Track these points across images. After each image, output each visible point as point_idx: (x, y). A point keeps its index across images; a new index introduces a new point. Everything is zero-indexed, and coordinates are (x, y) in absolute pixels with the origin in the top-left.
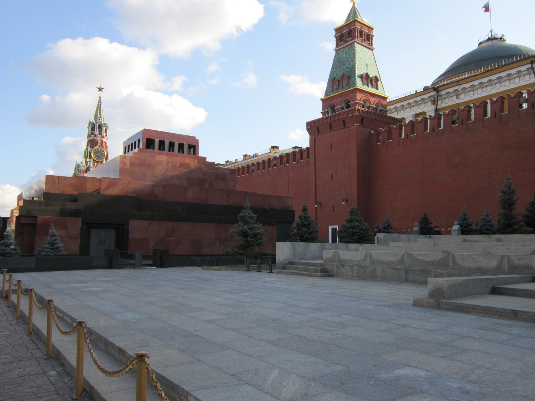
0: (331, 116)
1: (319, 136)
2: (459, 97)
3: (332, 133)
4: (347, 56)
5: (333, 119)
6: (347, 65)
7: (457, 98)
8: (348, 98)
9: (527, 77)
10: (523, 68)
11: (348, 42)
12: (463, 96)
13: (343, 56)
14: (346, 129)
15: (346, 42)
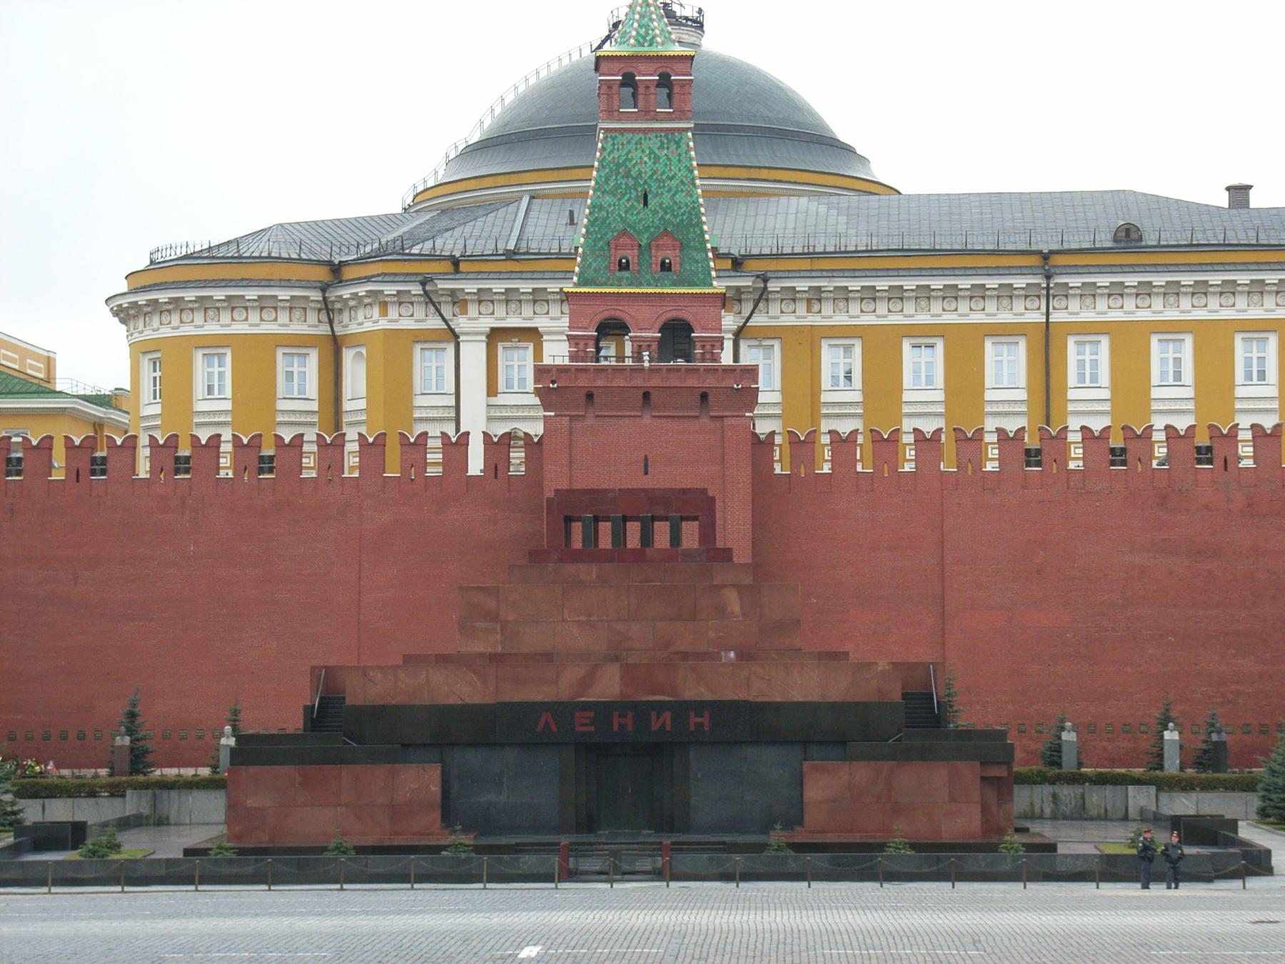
0: (651, 370)
1: (590, 421)
2: (816, 307)
3: (647, 420)
4: (660, 167)
5: (654, 382)
6: (666, 199)
7: (809, 311)
8: (688, 314)
9: (1019, 306)
10: (1019, 282)
11: (656, 120)
12: (827, 308)
13: (642, 162)
14: (705, 420)
15: (647, 114)
